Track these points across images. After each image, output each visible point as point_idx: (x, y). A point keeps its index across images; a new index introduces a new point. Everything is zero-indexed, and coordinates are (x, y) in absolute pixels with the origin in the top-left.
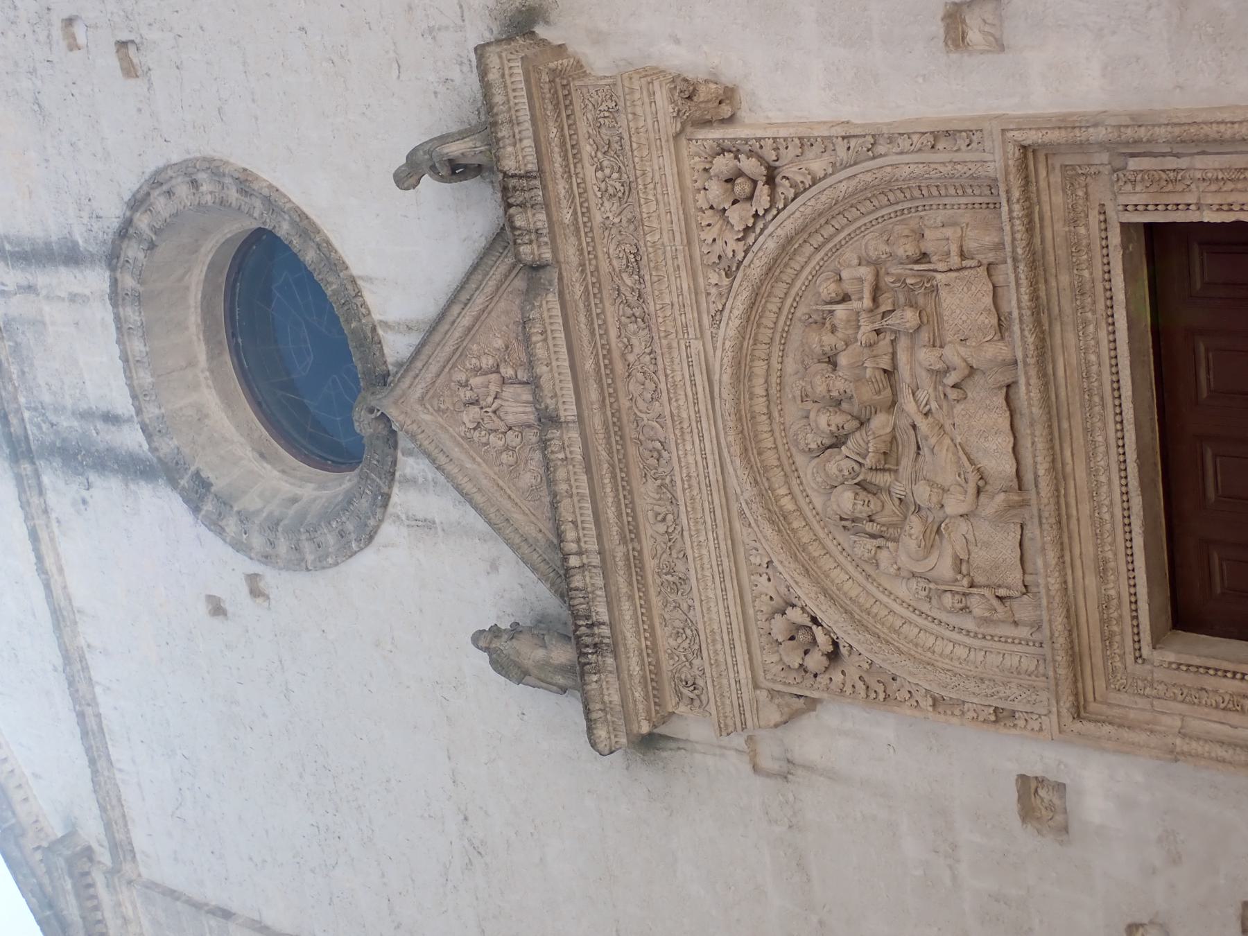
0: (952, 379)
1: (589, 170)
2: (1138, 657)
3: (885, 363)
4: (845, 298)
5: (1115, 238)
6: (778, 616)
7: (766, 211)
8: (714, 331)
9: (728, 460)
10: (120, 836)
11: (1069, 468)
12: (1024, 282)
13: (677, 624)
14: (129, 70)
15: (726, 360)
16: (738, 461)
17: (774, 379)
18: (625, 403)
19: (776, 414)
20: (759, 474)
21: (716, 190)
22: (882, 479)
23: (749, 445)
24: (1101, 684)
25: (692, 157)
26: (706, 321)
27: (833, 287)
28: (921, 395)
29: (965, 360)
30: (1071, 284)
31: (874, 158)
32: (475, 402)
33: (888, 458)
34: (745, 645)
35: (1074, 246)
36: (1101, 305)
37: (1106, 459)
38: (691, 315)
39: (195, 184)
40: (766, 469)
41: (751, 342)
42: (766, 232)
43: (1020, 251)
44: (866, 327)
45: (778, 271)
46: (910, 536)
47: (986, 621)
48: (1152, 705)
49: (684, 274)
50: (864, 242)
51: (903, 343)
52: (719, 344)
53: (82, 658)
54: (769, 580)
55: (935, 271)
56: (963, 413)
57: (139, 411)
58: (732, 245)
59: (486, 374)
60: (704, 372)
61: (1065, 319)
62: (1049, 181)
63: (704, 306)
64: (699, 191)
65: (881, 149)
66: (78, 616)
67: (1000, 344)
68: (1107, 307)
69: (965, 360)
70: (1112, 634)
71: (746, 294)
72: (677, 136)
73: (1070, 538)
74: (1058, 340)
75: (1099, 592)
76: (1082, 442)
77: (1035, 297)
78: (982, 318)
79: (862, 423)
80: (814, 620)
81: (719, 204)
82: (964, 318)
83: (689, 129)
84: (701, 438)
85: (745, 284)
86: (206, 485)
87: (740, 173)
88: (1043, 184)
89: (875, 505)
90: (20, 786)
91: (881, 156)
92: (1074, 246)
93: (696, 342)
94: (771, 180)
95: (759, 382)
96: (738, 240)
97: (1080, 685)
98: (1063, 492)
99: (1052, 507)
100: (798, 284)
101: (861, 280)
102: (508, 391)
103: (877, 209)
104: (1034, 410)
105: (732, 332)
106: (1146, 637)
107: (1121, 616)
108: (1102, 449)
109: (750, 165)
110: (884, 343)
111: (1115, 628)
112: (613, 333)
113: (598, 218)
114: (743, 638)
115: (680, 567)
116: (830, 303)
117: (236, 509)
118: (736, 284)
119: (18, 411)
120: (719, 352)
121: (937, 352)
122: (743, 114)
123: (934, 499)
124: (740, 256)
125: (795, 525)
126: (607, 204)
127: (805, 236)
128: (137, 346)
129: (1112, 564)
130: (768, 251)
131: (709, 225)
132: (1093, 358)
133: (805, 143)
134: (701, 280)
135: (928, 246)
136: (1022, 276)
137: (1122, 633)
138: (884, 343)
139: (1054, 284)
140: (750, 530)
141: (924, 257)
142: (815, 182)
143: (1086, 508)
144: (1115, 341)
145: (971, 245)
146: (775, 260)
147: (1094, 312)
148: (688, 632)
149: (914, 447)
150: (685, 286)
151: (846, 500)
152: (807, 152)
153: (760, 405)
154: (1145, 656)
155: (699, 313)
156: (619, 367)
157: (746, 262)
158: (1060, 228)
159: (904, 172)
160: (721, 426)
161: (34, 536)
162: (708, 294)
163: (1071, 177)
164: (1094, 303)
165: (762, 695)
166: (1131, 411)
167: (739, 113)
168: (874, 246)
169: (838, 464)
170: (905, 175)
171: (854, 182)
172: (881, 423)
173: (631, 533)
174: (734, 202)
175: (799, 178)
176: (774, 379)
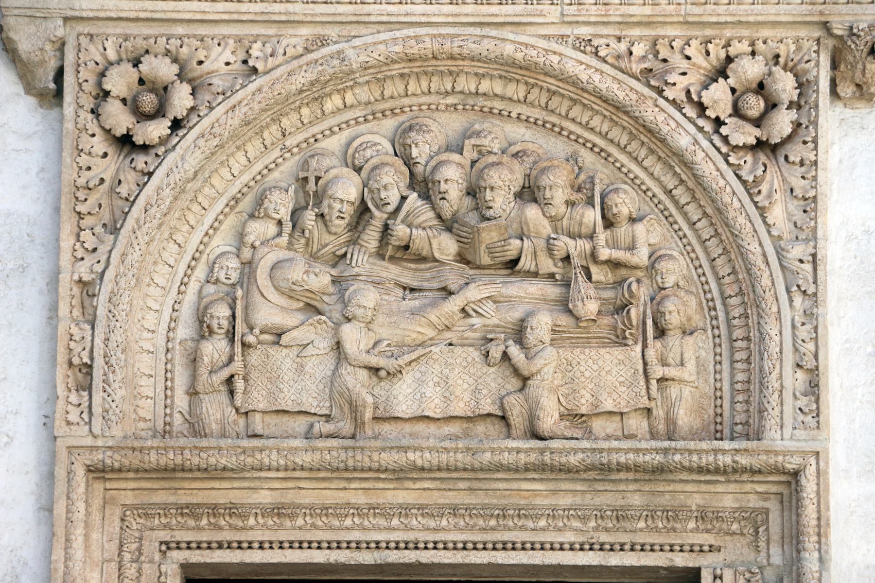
2: (167, 546)
4: (609, 223)
6: (175, 69)
7: (725, 139)
8: (570, 40)
9: (398, 34)
11: (409, 484)
15: (534, 53)
16: (398, 49)
17: (498, 105)
22: (371, 237)
24: (129, 498)
25: (797, 41)
26: (584, 31)
27: (625, 211)
28: (489, 306)
29: (539, 372)
30: (629, 508)
31: (788, 291)
34: (132, 15)
36: (604, 537)
40: (381, 81)
41: (553, 88)
42: (700, 137)
43: (677, 457)
44: (577, 248)
45: (646, 140)
46: (306, 272)
48: (109, 561)
50: (675, 253)
52: (554, 46)
54: (228, 64)
55: (645, 346)
56: (469, 359)
58: (682, 82)
60: (516, 19)
61: (589, 496)
63: (604, 31)
64: (752, 44)
65: (798, 300)
67: (556, 416)
68: (602, 544)
69: (539, 372)
70: (197, 517)
71: (621, 95)
72: (825, 26)
73: (324, 479)
74: (564, 486)
75: (252, 506)
76: (442, 501)
77: (621, 468)
78: (588, 396)
79: (448, 225)
81: (735, 72)
82: (587, 374)
83: (830, 43)
85: (634, 97)
87: (772, 106)
91: (791, 301)
93: (558, 14)
95: (498, 87)
96: (688, 92)
97: (131, 475)
98: (383, 476)
99: (367, 463)
100: (623, 158)
101: (632, 247)
103: (719, 279)
104: (488, 455)
107: (220, 528)
108: (432, 523)
111: (204, 522)
114: (142, 15)
116: (602, 203)
118: (634, 83)
120: (543, 44)
121: (547, 338)
122: (839, 107)
123: (360, 312)
124: (669, 93)
125: (305, 111)
127: (691, 184)
129: (288, 523)
130: (676, 135)
131: (708, 53)
132: (542, 523)
135: (673, 340)
136: (648, 458)
137: (199, 528)
139: (631, 487)
140: (300, 50)
142: (762, 211)
143: (361, 499)
144: (561, 549)
145: (674, 391)
146: (663, 141)
147: (596, 529)
149: (415, 284)
150: (632, 10)
152: (796, 202)
153: (466, 84)
154: (169, 554)
155: (595, 23)
157: (661, 102)
159: (771, 328)
160: (444, 31)
162: (619, 39)
164: (607, 530)
166: (478, 561)
167: (840, 104)
170: (767, 327)
171: (760, 262)
174: (733, 90)
175: (764, 188)
176: (498, 105)
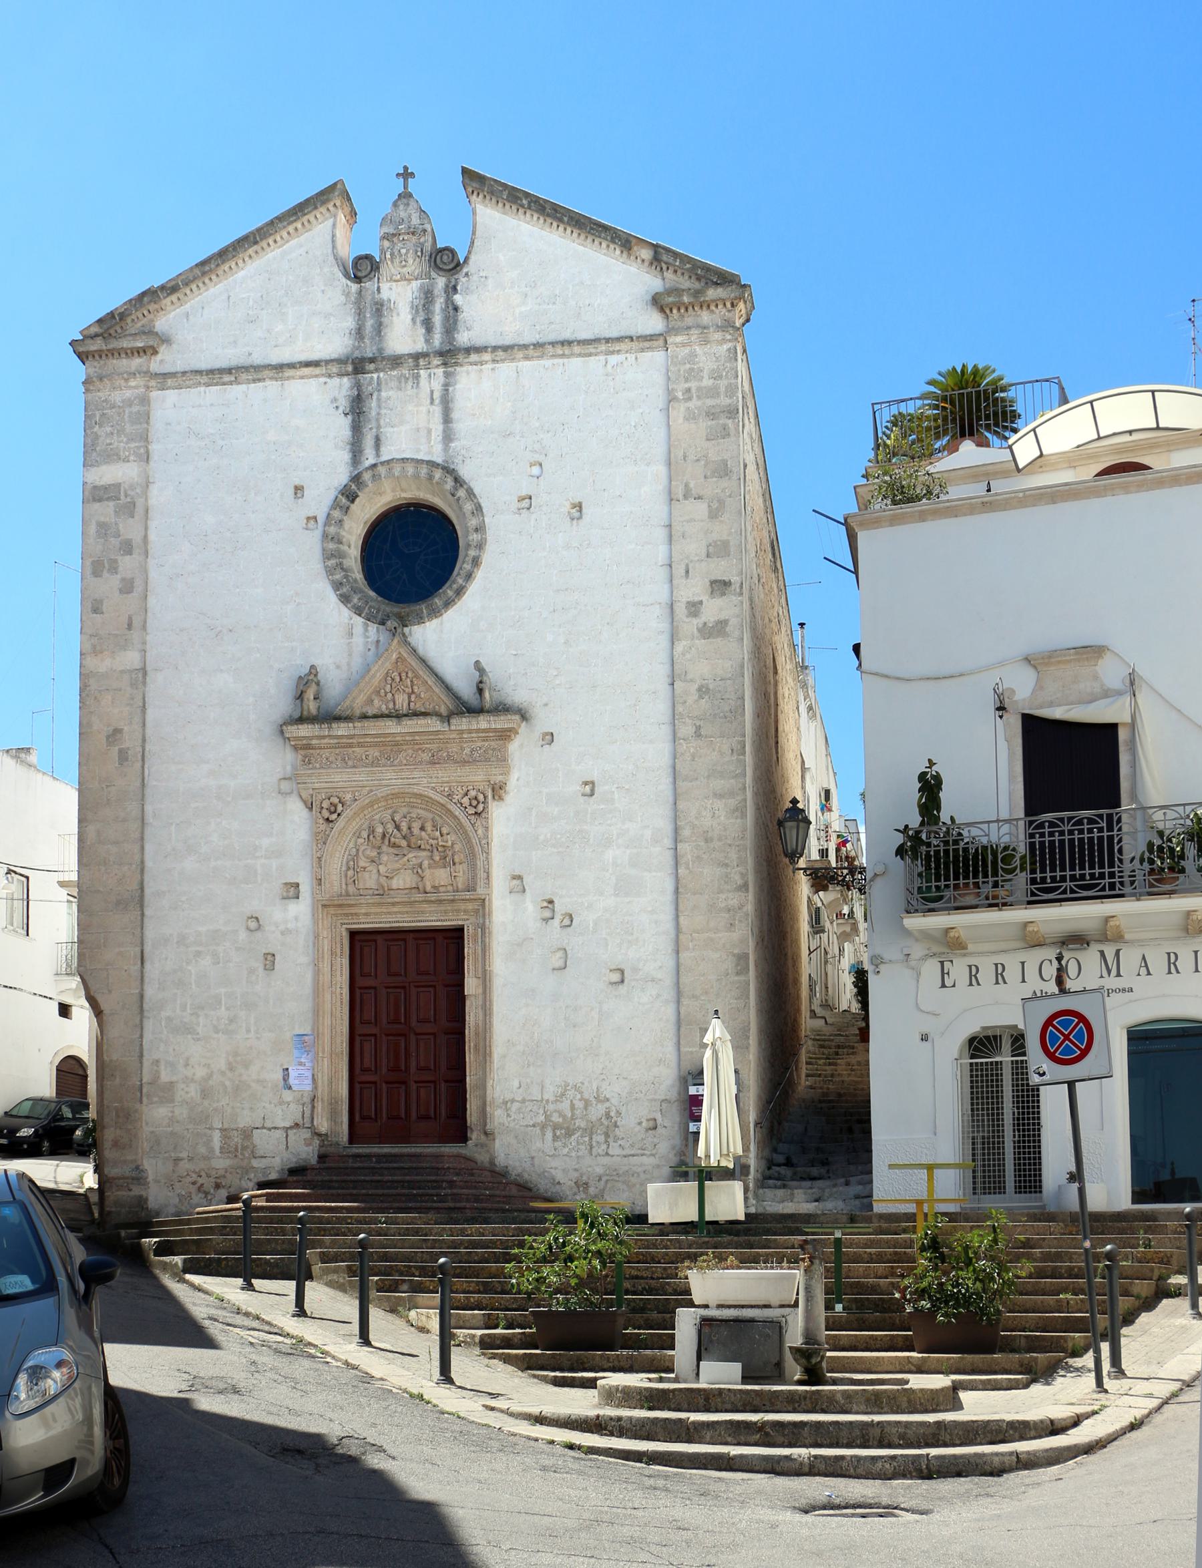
0: (419, 871)
1: (479, 744)
3: (422, 847)
4: (442, 835)
5: (460, 923)
18: (404, 747)
20: (385, 798)
21: (473, 793)
22: (386, 842)
23: (395, 796)
24: (333, 912)
32: (401, 680)
33: (394, 846)
35: (458, 911)
37: (399, 917)
38: (435, 780)
39: (476, 530)
47: (346, 876)
51: (429, 854)
53: (259, 380)
57: (382, 463)
66: (280, 383)
79: (404, 837)
80: (339, 815)
86: (353, 501)
87: (478, 803)
90: (179, 299)
92: (458, 911)
102: (406, 697)
109: (480, 807)
115: (350, 763)
117: (345, 518)
119: (377, 370)
133: (487, 829)
135: (457, 866)
138: (428, 847)
141: (454, 864)
145: (458, 879)
151: (380, 830)
156: (417, 747)
158: (463, 908)
161: (315, 364)
163: (476, 911)
165: (311, 792)
168: (457, 847)
169: (390, 827)
172: (404, 843)
173: (360, 745)
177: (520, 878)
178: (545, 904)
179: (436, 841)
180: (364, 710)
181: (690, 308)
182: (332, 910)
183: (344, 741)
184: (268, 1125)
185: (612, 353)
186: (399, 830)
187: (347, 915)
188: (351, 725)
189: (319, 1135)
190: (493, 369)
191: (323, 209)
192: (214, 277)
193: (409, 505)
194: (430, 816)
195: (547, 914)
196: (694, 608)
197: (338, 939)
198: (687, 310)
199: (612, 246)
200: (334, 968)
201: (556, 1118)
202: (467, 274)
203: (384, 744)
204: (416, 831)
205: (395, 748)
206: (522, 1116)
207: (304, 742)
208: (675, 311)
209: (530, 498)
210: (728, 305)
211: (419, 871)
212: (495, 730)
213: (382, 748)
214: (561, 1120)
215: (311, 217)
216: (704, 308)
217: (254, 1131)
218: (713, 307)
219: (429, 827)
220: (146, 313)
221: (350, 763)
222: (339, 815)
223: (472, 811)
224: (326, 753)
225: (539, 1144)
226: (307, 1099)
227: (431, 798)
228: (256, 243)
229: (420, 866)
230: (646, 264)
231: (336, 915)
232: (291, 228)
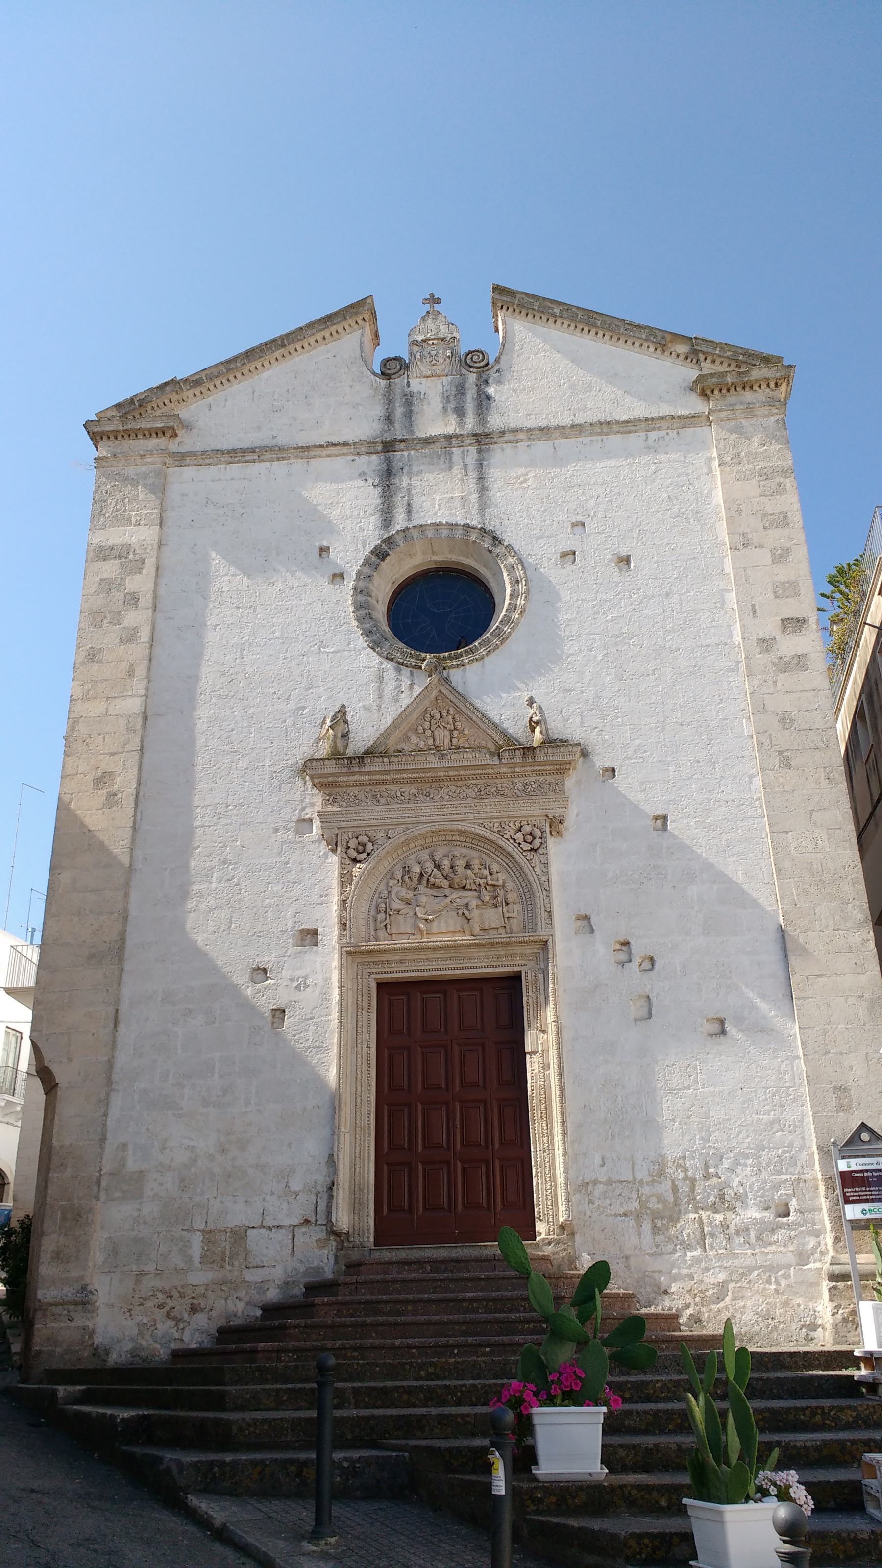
0: (466, 912)
1: (533, 779)
4: (491, 874)
5: (516, 969)
10: (188, 460)
12: (503, 940)
13: (360, 797)
14: (564, 555)
19: (445, 843)
20: (424, 836)
21: (527, 829)
22: (424, 882)
26: (481, 821)
32: (441, 717)
33: (434, 886)
35: (513, 956)
36: (494, 964)
37: (441, 964)
44: (482, 881)
49: (498, 814)
51: (476, 894)
53: (284, 458)
58: (509, 833)
59: (454, 723)
62: (534, 949)
65: (544, 892)
71: (492, 838)
72: (547, 816)
74: (481, 950)
80: (368, 854)
84: (437, 815)
86: (383, 559)
87: (534, 838)
88: (533, 947)
89: (415, 880)
92: (513, 956)
94: (532, 849)
100: (494, 856)
102: (447, 733)
105: (478, 831)
106: (379, 976)
109: (537, 842)
110: (474, 887)
112: (473, 782)
113: (516, 780)
117: (375, 574)
119: (407, 449)
122: (553, 838)
126: (521, 784)
128: (445, 532)
133: (546, 865)
134: (495, 820)
135: (510, 906)
138: (474, 887)
141: (507, 904)
143: (424, 957)
148: (357, 801)
151: (417, 869)
156: (459, 783)
158: (519, 952)
161: (345, 444)
165: (336, 831)
168: (510, 885)
169: (429, 866)
172: (445, 883)
173: (395, 782)
176: (458, 843)
177: (587, 918)
178: (618, 947)
179: (485, 880)
180: (399, 747)
181: (732, 389)
182: (359, 959)
183: (377, 777)
184: (269, 1222)
185: (654, 429)
186: (439, 869)
187: (375, 963)
188: (386, 760)
189: (337, 1234)
190: (528, 446)
191: (351, 322)
192: (239, 375)
193: (437, 570)
194: (474, 854)
195: (622, 956)
196: (766, 644)
197: (365, 991)
198: (728, 390)
199: (645, 344)
200: (360, 1024)
201: (653, 1204)
202: (498, 371)
203: (423, 781)
204: (460, 870)
205: (435, 785)
206: (608, 1201)
207: (330, 779)
208: (716, 392)
209: (574, 553)
210: (772, 385)
211: (466, 912)
212: (552, 764)
213: (420, 785)
214: (660, 1206)
215: (339, 328)
216: (747, 389)
217: (249, 1232)
218: (756, 387)
219: (476, 864)
220: (167, 402)
221: (383, 801)
222: (368, 854)
223: (527, 847)
224: (354, 791)
225: (635, 1240)
226: (322, 1188)
227: (478, 835)
228: (283, 346)
229: (467, 906)
230: (682, 358)
231: (363, 964)
232: (319, 336)
